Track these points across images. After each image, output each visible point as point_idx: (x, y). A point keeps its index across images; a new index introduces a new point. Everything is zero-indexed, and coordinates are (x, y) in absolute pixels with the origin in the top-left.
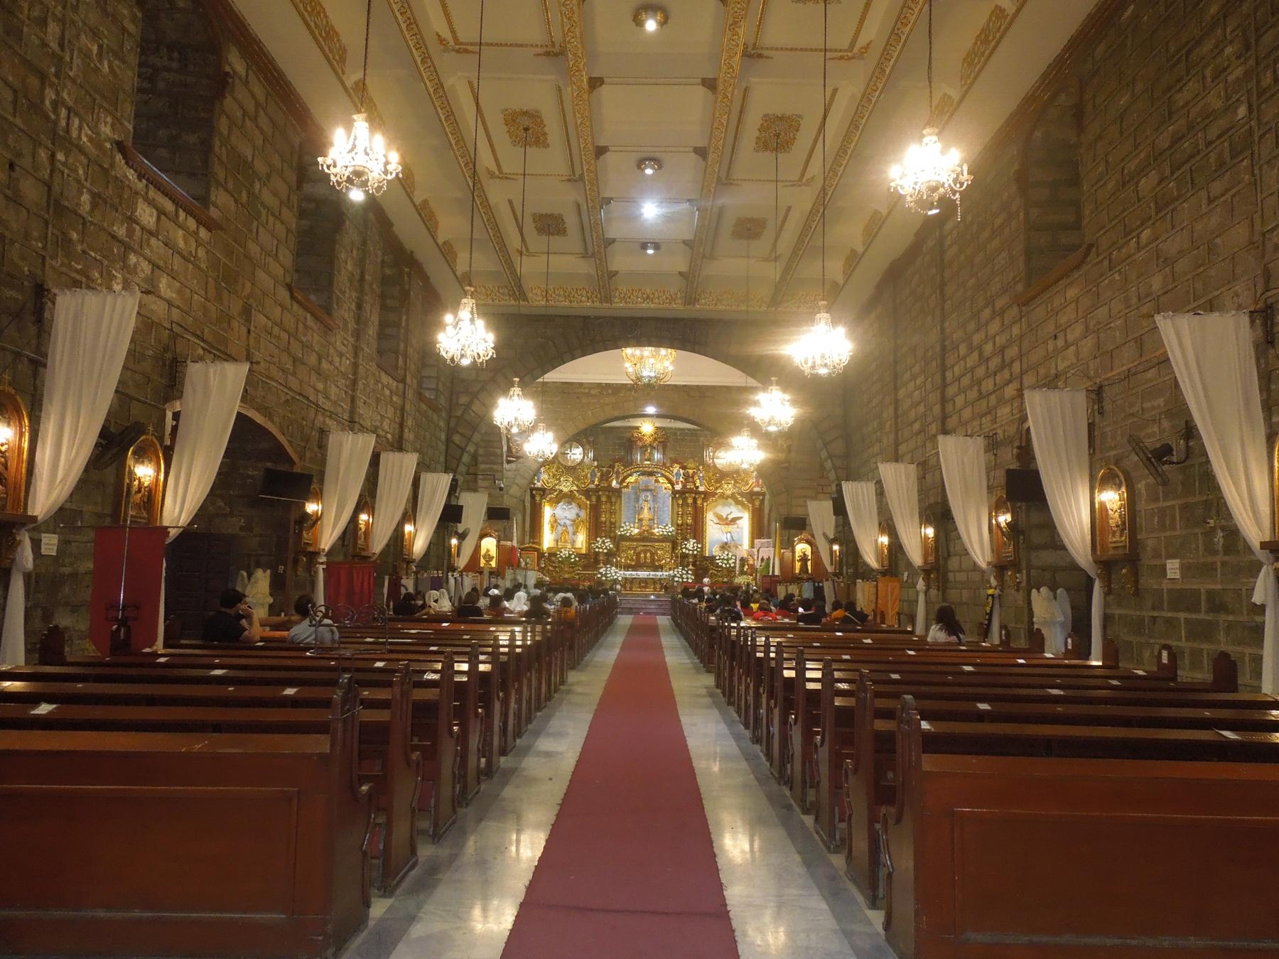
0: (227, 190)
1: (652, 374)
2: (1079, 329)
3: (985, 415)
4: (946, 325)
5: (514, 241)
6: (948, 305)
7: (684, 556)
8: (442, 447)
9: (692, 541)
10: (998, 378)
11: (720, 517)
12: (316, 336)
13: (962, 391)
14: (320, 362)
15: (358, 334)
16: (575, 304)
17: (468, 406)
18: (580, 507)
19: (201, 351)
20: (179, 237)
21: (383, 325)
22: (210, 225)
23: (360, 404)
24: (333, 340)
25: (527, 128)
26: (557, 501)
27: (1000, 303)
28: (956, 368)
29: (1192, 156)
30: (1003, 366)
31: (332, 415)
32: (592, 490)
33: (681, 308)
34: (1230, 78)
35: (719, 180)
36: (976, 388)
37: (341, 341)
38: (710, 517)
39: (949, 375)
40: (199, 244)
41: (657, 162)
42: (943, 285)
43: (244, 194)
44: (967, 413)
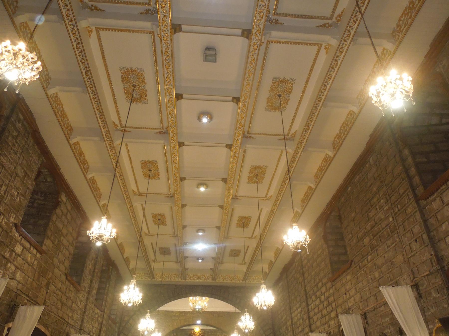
0: (51, 240)
1: (200, 307)
2: (353, 291)
3: (325, 324)
4: (306, 288)
5: (152, 257)
6: (306, 281)
10: (328, 309)
12: (73, 294)
13: (315, 314)
14: (72, 304)
15: (89, 293)
16: (172, 280)
17: (128, 321)
19: (26, 301)
20: (29, 257)
21: (99, 289)
22: (41, 252)
23: (85, 321)
24: (79, 295)
25: (159, 219)
27: (324, 281)
28: (312, 305)
29: (379, 233)
30: (329, 304)
31: (73, 326)
33: (211, 281)
34: (385, 209)
35: (224, 237)
36: (320, 313)
37: (82, 295)
39: (310, 307)
40: (35, 259)
41: (203, 231)
42: (303, 274)
43: (57, 241)
44: (318, 323)
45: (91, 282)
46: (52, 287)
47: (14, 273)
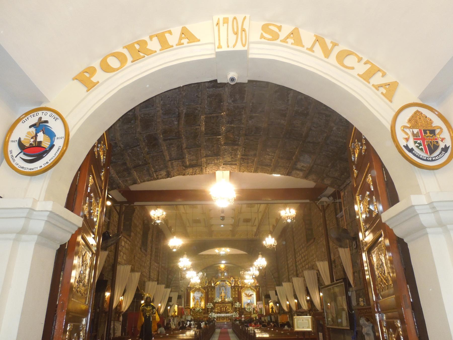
1: (224, 253)
7: (236, 308)
8: (166, 280)
9: (238, 303)
11: (246, 295)
15: (151, 255)
18: (202, 293)
21: (156, 252)
23: (151, 272)
26: (194, 292)
30: (305, 260)
32: (205, 287)
38: (243, 295)
45: (152, 248)
46: (136, 258)
47: (123, 256)
